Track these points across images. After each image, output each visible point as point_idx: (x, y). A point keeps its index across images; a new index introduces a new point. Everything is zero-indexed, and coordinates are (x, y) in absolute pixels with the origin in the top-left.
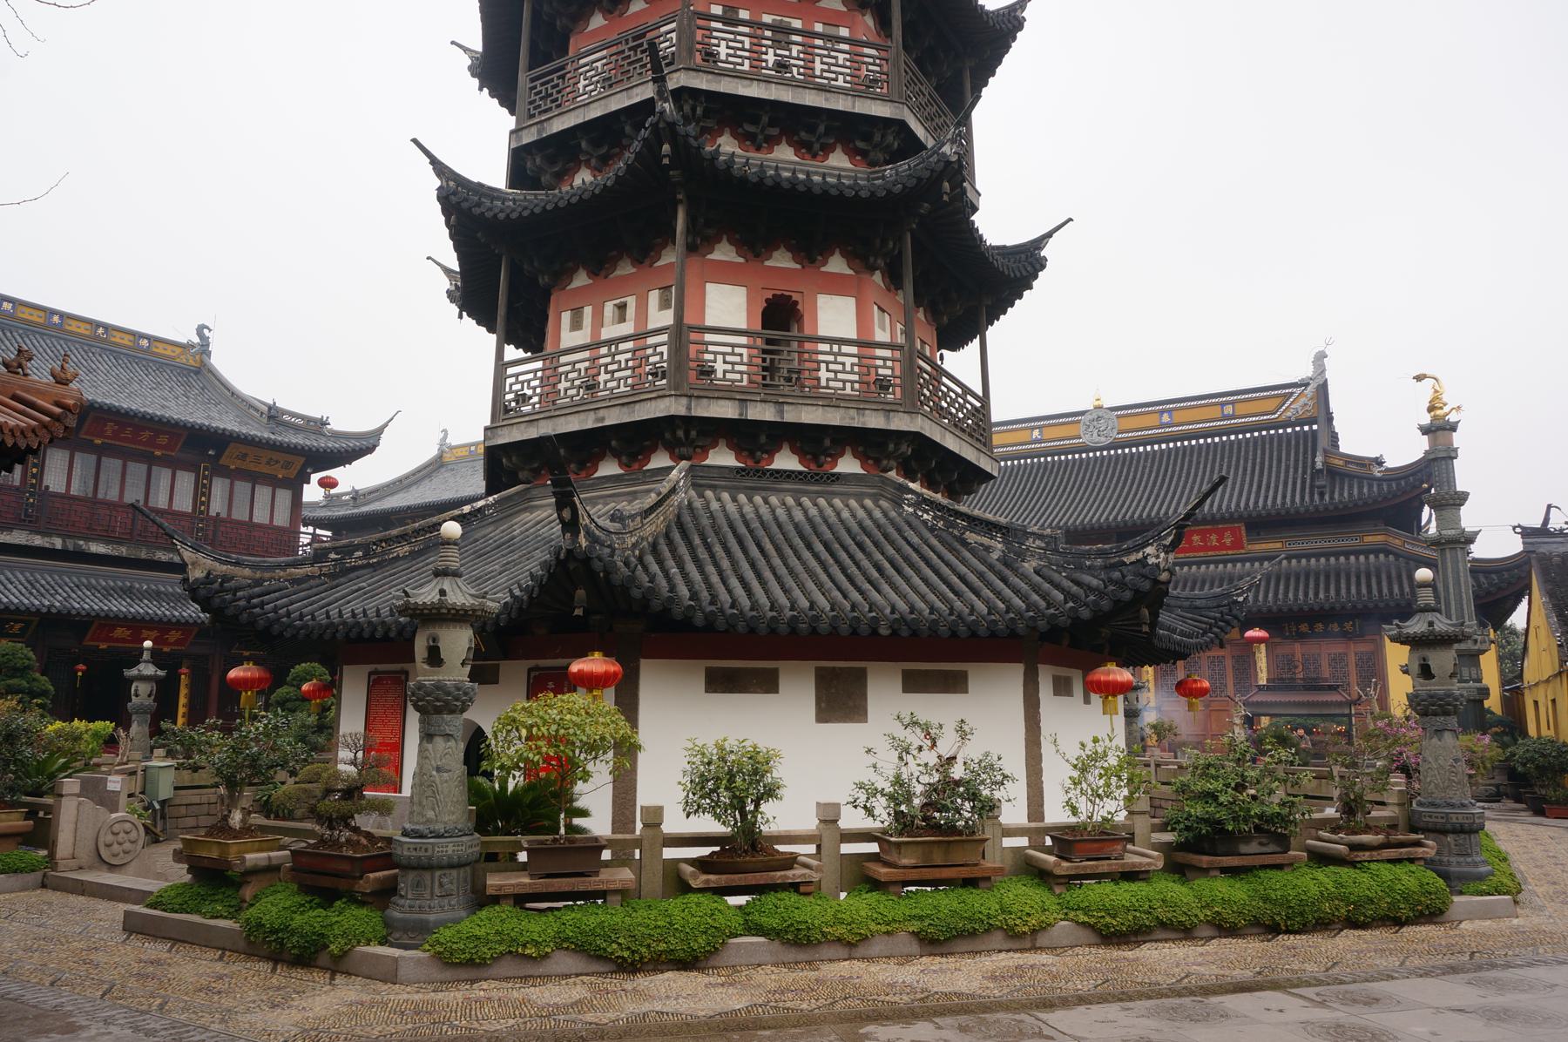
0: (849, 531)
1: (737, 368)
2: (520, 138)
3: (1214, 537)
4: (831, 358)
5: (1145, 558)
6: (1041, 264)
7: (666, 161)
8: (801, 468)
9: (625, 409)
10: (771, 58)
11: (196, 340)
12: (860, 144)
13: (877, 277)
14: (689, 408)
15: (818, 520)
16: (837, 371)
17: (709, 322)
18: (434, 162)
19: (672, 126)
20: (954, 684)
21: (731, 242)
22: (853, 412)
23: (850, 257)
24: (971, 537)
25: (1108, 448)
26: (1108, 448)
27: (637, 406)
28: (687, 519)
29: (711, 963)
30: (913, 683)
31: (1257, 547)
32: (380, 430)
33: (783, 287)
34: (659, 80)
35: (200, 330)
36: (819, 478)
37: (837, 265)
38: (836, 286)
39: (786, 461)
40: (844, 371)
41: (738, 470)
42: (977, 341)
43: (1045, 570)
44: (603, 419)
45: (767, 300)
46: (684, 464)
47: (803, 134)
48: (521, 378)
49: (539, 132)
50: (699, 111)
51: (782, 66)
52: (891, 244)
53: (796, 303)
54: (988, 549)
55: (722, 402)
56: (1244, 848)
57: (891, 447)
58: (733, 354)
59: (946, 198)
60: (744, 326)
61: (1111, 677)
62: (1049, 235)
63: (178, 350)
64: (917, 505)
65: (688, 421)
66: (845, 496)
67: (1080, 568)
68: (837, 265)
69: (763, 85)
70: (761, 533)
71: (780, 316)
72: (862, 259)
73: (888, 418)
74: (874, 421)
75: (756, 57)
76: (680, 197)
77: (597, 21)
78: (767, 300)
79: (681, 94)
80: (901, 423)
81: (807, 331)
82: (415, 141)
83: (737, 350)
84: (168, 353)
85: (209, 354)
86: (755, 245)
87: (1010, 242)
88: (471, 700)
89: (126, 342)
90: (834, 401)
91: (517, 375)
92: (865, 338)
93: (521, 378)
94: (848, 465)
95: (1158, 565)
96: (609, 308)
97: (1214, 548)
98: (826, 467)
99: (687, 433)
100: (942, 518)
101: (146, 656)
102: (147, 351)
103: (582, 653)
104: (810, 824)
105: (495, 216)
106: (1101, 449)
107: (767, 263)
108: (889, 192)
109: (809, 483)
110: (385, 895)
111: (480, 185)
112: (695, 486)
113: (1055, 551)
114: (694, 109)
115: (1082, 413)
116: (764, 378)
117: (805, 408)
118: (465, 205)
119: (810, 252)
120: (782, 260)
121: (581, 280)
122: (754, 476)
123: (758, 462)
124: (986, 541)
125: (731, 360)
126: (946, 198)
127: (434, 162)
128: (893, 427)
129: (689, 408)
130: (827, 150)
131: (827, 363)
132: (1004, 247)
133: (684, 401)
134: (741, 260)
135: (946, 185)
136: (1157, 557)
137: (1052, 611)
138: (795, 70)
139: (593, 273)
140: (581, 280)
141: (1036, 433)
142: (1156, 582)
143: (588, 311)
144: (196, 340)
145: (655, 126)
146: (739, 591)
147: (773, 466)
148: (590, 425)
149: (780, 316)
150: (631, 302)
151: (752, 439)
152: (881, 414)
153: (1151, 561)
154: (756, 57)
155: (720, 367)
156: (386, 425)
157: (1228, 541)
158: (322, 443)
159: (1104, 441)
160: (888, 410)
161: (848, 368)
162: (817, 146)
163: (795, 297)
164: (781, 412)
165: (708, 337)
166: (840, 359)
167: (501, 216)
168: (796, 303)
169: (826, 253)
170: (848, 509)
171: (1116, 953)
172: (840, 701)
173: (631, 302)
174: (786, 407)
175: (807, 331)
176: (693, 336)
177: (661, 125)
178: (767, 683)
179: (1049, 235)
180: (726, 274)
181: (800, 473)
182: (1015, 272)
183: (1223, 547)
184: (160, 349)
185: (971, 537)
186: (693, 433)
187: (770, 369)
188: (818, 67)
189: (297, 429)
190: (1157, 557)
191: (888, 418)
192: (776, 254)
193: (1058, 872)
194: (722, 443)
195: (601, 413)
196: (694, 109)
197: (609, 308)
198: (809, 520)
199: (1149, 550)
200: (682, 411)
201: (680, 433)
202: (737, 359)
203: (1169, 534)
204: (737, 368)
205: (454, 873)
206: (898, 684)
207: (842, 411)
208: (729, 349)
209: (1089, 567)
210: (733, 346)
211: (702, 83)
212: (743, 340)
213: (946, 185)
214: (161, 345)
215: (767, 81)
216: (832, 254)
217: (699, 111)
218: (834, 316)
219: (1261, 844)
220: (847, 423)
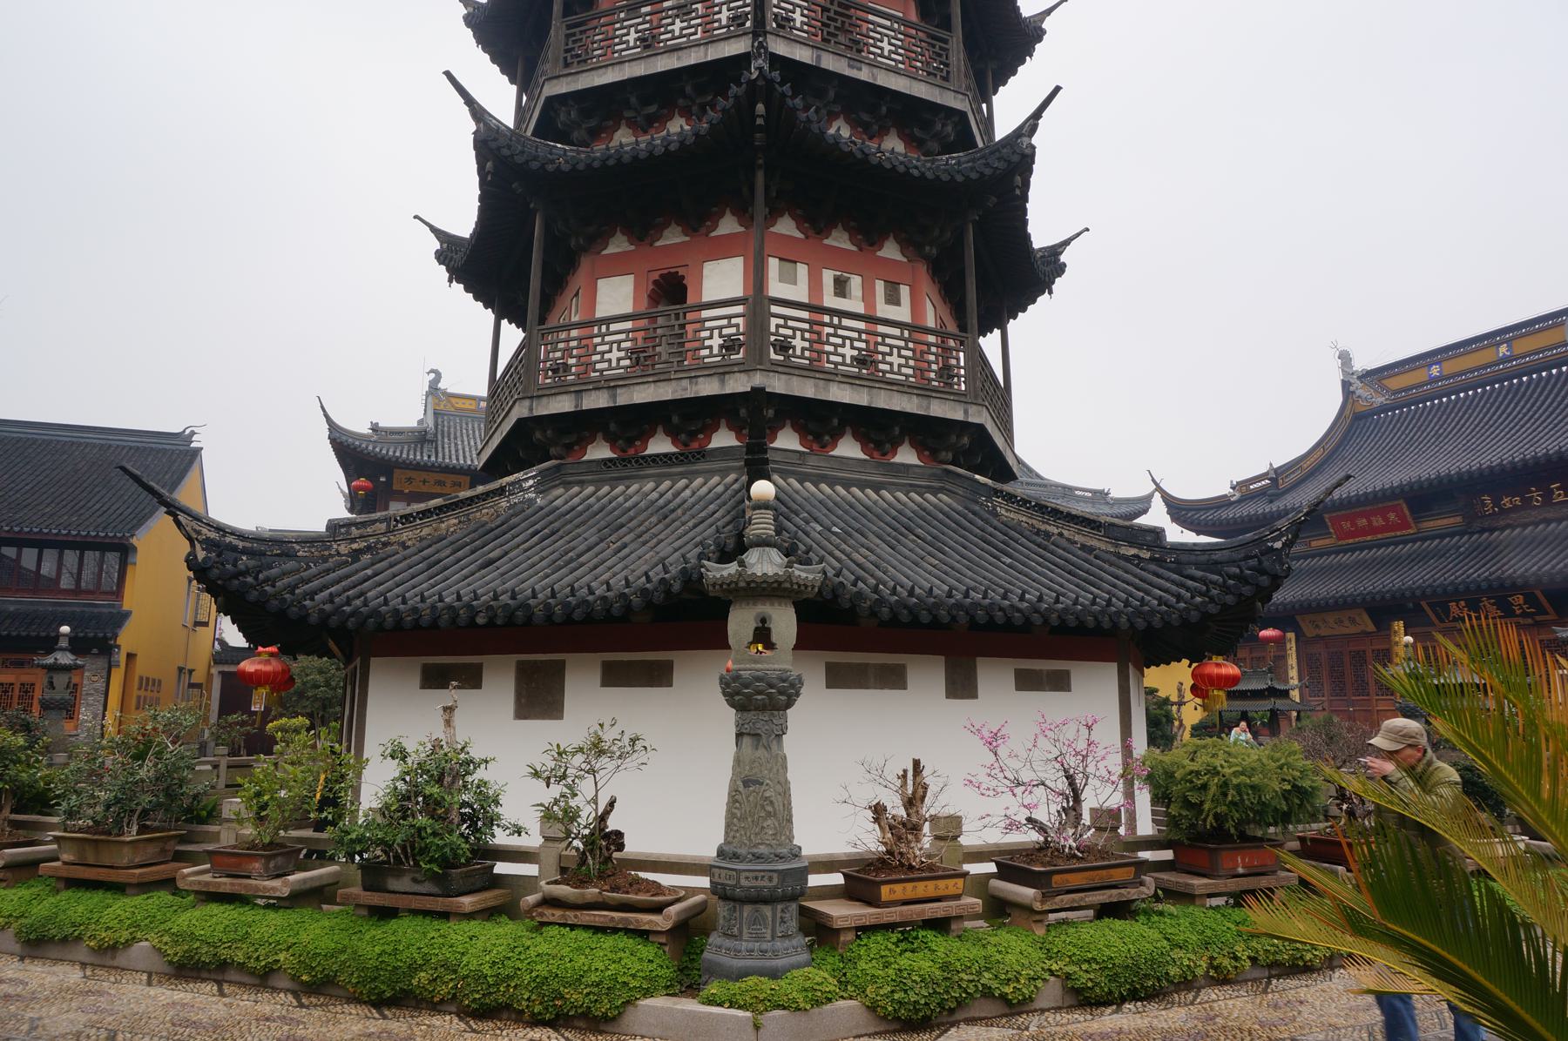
0: (941, 511)
14: (531, 409)
18: (434, 230)
20: (658, 676)
22: (685, 383)
30: (615, 676)
37: (728, 226)
38: (723, 249)
55: (559, 398)
56: (393, 884)
60: (806, 300)
68: (728, 226)
69: (617, 68)
73: (723, 382)
78: (655, 282)
86: (643, 232)
107: (658, 244)
109: (674, 465)
117: (637, 388)
119: (697, 220)
127: (434, 230)
128: (728, 391)
129: (531, 409)
133: (527, 403)
141: (1503, 349)
147: (647, 452)
151: (629, 425)
163: (681, 272)
164: (614, 397)
172: (539, 697)
174: (619, 391)
178: (472, 679)
180: (616, 267)
191: (723, 382)
192: (666, 233)
200: (525, 413)
206: (417, 680)
207: (674, 383)
216: (722, 215)
219: (415, 880)
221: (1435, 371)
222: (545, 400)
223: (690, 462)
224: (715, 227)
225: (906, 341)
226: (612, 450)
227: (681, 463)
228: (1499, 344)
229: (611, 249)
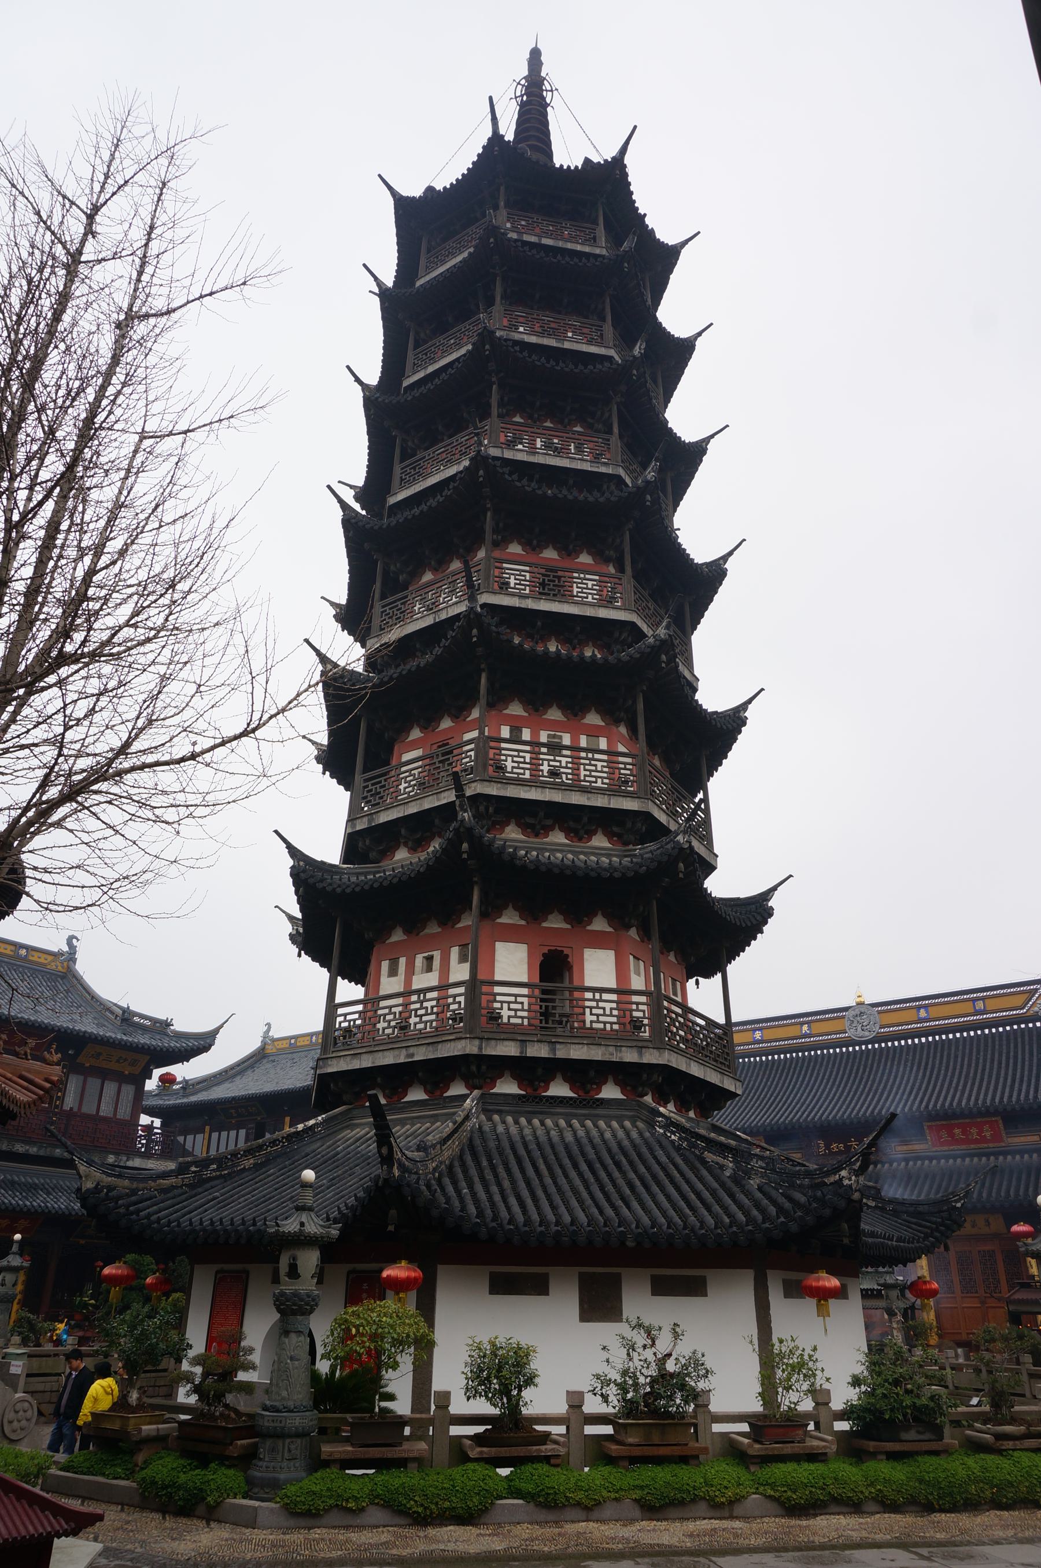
1: (519, 1013)
2: (354, 826)
3: (974, 1130)
4: (594, 1004)
5: (841, 1179)
6: (769, 913)
7: (465, 856)
8: (572, 1094)
9: (430, 1048)
10: (545, 768)
11: (66, 949)
12: (615, 829)
13: (633, 933)
14: (480, 1048)
15: (585, 1141)
16: (600, 1013)
17: (498, 977)
18: (290, 847)
19: (470, 830)
20: (695, 1288)
21: (515, 909)
22: (611, 1049)
23: (610, 918)
24: (709, 1157)
25: (872, 1041)
26: (872, 1041)
27: (440, 1046)
28: (477, 1142)
29: (482, 1520)
30: (662, 1288)
31: (1016, 1140)
32: (216, 1031)
33: (556, 943)
34: (459, 788)
35: (70, 940)
36: (586, 1102)
37: (599, 924)
38: (599, 942)
39: (559, 1089)
40: (604, 1015)
42: (719, 975)
43: (766, 1188)
44: (412, 1055)
45: (544, 955)
46: (476, 1093)
47: (571, 823)
48: (349, 1017)
49: (369, 822)
50: (491, 810)
51: (554, 773)
52: (641, 909)
53: (567, 956)
54: (722, 1167)
55: (506, 1043)
56: (904, 1436)
57: (645, 1076)
58: (516, 1002)
59: (681, 875)
61: (821, 1283)
62: (774, 889)
63: (50, 958)
64: (666, 1127)
65: (480, 1058)
66: (608, 1119)
67: (792, 1186)
68: (599, 924)
69: (539, 790)
70: (537, 1154)
71: (554, 970)
72: (620, 920)
73: (641, 1054)
74: (629, 1056)
75: (535, 767)
76: (475, 879)
77: (416, 734)
78: (544, 955)
79: (477, 799)
80: (651, 1057)
81: (576, 983)
82: (276, 832)
83: (519, 999)
84: (42, 960)
85: (74, 961)
87: (743, 895)
88: (317, 1305)
89: (8, 952)
90: (594, 1037)
91: (345, 1015)
92: (624, 987)
93: (349, 1017)
94: (610, 1092)
95: (850, 1186)
96: (419, 960)
97: (976, 1141)
98: (592, 1093)
99: (479, 1068)
100: (686, 1139)
101: (15, 1248)
102: (25, 959)
103: (393, 1260)
104: (560, 1408)
105: (334, 889)
106: (866, 1043)
107: (544, 925)
108: (636, 872)
109: (577, 1107)
110: (249, 1458)
111: (322, 862)
112: (485, 1111)
113: (773, 1170)
114: (487, 808)
115: (846, 1009)
116: (541, 1021)
117: (573, 1046)
118: (311, 881)
120: (555, 922)
121: (398, 936)
122: (533, 1102)
123: (535, 1090)
124: (720, 1160)
125: (513, 1005)
126: (681, 875)
127: (290, 847)
128: (645, 1061)
129: (480, 1048)
130: (590, 834)
131: (591, 1008)
132: (738, 899)
133: (477, 1042)
134: (523, 923)
135: (681, 865)
136: (850, 1179)
137: (767, 1225)
138: (564, 776)
139: (407, 931)
140: (398, 936)
141: (805, 1028)
142: (850, 1201)
143: (403, 961)
144: (66, 949)
145: (456, 830)
146: (519, 1208)
148: (402, 1059)
149: (554, 970)
150: (437, 955)
152: (635, 1050)
153: (846, 1182)
154: (535, 767)
155: (505, 1013)
156: (221, 1026)
157: (988, 1134)
158: (166, 1043)
159: (868, 1035)
160: (641, 1046)
161: (608, 1012)
162: (582, 832)
163: (566, 951)
164: (554, 1050)
165: (497, 989)
166: (601, 1004)
167: (339, 890)
168: (567, 956)
169: (591, 916)
170: (611, 1130)
171: (794, 1522)
172: (600, 1304)
173: (437, 955)
174: (558, 1046)
175: (576, 983)
176: (485, 989)
177: (462, 830)
178: (539, 1287)
179: (774, 889)
180: (511, 935)
181: (571, 1098)
182: (749, 918)
183: (984, 1140)
184: (35, 957)
185: (709, 1157)
186: (484, 1068)
187: (546, 1014)
188: (583, 773)
189: (144, 1029)
190: (850, 1179)
191: (641, 1054)
193: (751, 1452)
194: (507, 1074)
195: (411, 1050)
196: (487, 808)
197: (419, 960)
198: (577, 1140)
199: (844, 1173)
200: (475, 1050)
201: (474, 1068)
202: (519, 1006)
203: (857, 1160)
204: (519, 1013)
205: (299, 1441)
207: (603, 1048)
208: (512, 999)
209: (800, 1186)
210: (516, 996)
211: (493, 790)
212: (525, 991)
213: (681, 865)
214: (36, 954)
215: (543, 786)
216: (596, 915)
217: (491, 810)
218: (598, 968)
219: (918, 1432)
220: (607, 1058)
221: (758, 1035)
222: (493, 1042)
223: (591, 1107)
224: (590, 923)
225: (597, 1001)
226: (520, 1087)
227: (585, 1107)
228: (802, 1024)
229: (504, 920)
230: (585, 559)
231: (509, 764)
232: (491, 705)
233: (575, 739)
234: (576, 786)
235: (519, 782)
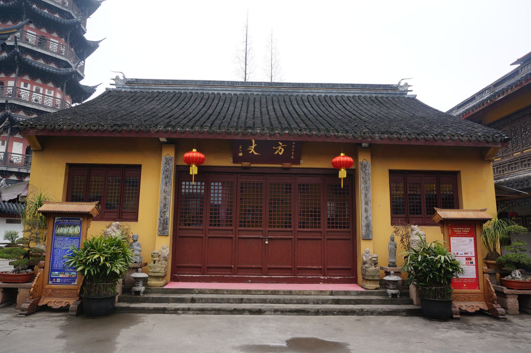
10: (34, 99)
41: (17, 180)
46: (4, 179)
51: (36, 100)
65: (6, 171)
75: (30, 97)
112: (6, 183)
154: (30, 97)
165: (12, 155)
176: (9, 155)
180: (18, 140)
187: (26, 162)
188: (45, 102)
200: (5, 169)
211: (17, 103)
212: (21, 156)
215: (33, 104)
230: (55, 35)
231: (23, 96)
232: (19, 75)
233: (44, 91)
234: (42, 105)
235: (25, 101)
